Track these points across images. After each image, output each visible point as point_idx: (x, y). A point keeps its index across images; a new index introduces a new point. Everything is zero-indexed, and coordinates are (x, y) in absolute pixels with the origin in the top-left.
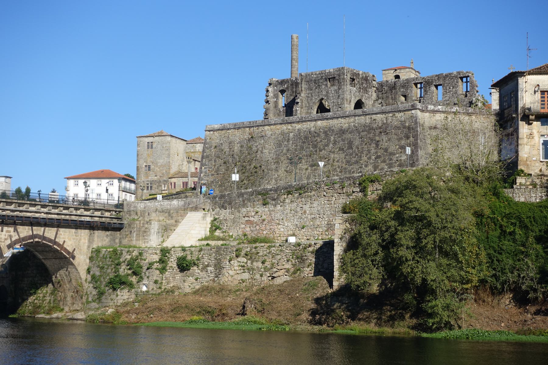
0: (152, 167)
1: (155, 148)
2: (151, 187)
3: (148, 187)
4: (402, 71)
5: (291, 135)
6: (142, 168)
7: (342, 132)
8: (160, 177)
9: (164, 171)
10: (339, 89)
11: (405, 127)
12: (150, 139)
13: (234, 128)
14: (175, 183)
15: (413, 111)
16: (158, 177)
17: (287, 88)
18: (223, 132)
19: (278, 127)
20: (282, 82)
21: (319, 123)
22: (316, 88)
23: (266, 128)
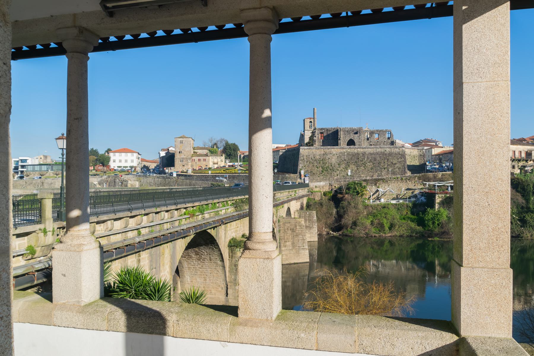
0: (183, 152)
2: (183, 161)
3: (181, 161)
7: (371, 154)
10: (360, 136)
11: (399, 154)
12: (181, 139)
13: (316, 149)
14: (194, 159)
15: (403, 149)
17: (324, 131)
20: (322, 129)
21: (359, 150)
22: (348, 134)
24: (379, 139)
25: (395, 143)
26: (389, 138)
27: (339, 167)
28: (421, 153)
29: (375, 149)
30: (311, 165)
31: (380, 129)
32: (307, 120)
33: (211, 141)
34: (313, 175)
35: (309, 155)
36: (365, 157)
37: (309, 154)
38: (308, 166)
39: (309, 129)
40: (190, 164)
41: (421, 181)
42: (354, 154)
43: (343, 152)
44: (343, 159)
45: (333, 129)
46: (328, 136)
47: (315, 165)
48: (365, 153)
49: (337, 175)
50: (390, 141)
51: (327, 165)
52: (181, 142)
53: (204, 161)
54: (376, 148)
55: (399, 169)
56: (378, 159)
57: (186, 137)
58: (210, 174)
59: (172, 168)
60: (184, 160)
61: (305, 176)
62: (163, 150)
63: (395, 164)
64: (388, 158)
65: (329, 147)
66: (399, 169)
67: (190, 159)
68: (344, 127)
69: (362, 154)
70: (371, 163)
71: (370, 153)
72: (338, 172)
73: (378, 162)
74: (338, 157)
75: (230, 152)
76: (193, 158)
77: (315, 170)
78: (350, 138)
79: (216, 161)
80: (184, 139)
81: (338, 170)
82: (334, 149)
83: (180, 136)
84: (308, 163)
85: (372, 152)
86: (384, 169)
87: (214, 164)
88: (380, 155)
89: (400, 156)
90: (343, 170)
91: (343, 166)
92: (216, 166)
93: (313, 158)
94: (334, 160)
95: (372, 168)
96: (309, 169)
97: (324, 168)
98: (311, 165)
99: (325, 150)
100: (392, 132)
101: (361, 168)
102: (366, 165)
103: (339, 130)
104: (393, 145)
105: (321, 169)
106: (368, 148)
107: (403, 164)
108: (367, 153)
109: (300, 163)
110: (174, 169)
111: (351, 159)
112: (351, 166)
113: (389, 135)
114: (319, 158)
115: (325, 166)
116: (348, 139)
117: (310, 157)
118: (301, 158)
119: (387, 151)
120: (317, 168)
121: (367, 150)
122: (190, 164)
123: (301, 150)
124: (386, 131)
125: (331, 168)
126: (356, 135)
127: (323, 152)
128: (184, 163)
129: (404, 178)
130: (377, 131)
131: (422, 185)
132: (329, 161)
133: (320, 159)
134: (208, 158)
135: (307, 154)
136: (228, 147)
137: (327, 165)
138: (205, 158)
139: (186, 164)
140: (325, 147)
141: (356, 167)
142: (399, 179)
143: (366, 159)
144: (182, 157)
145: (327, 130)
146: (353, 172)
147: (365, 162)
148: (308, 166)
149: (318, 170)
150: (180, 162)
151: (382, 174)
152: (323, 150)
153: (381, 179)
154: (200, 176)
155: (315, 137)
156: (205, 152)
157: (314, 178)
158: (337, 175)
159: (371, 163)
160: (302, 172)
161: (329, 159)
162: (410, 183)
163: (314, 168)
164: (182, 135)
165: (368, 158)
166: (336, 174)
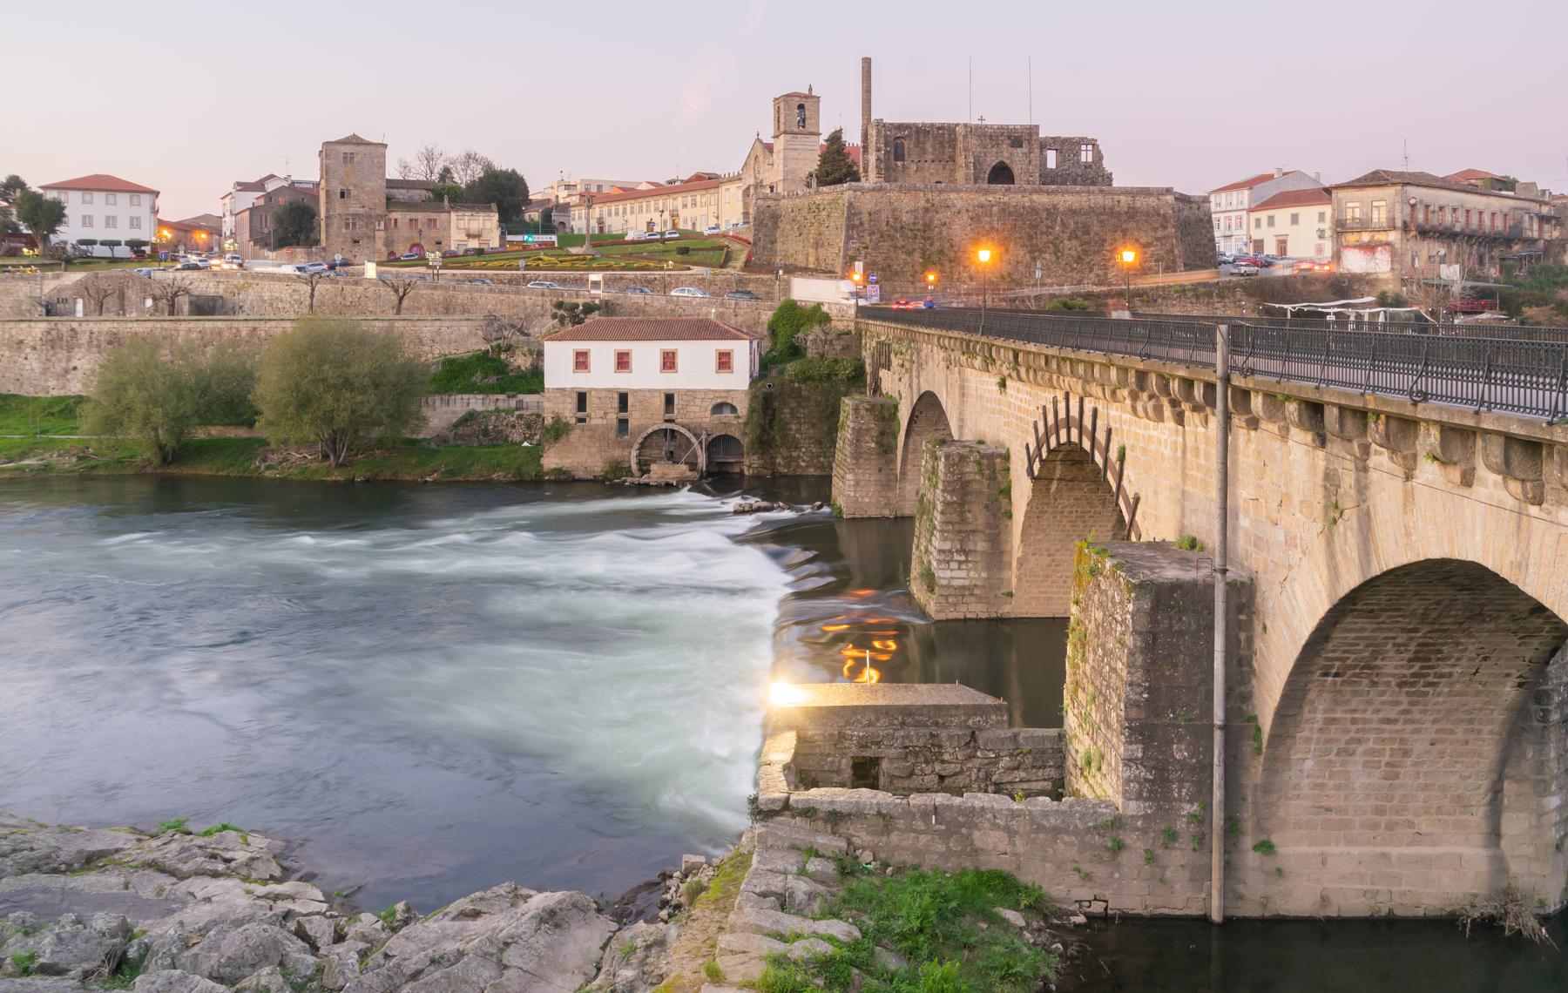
0: (354, 192)
1: (359, 163)
2: (354, 224)
3: (348, 224)
5: (995, 209)
6: (335, 194)
7: (1073, 212)
8: (370, 209)
9: (377, 201)
10: (1030, 153)
12: (348, 149)
14: (396, 220)
17: (909, 136)
21: (1035, 197)
22: (993, 147)
23: (953, 196)
31: (1064, 135)
36: (1056, 220)
43: (988, 203)
48: (1055, 207)
54: (1089, 192)
60: (360, 223)
67: (380, 218)
69: (1047, 210)
71: (1071, 210)
78: (1000, 159)
80: (361, 148)
85: (1076, 206)
87: (469, 236)
92: (474, 244)
95: (1079, 257)
101: (1044, 255)
108: (1061, 209)
113: (1090, 154)
116: (991, 161)
122: (380, 235)
127: (922, 203)
130: (1054, 139)
133: (915, 224)
134: (444, 216)
139: (368, 237)
141: (1030, 252)
143: (1057, 228)
144: (351, 210)
147: (1056, 239)
150: (344, 230)
151: (1109, 276)
159: (1075, 242)
165: (1063, 224)
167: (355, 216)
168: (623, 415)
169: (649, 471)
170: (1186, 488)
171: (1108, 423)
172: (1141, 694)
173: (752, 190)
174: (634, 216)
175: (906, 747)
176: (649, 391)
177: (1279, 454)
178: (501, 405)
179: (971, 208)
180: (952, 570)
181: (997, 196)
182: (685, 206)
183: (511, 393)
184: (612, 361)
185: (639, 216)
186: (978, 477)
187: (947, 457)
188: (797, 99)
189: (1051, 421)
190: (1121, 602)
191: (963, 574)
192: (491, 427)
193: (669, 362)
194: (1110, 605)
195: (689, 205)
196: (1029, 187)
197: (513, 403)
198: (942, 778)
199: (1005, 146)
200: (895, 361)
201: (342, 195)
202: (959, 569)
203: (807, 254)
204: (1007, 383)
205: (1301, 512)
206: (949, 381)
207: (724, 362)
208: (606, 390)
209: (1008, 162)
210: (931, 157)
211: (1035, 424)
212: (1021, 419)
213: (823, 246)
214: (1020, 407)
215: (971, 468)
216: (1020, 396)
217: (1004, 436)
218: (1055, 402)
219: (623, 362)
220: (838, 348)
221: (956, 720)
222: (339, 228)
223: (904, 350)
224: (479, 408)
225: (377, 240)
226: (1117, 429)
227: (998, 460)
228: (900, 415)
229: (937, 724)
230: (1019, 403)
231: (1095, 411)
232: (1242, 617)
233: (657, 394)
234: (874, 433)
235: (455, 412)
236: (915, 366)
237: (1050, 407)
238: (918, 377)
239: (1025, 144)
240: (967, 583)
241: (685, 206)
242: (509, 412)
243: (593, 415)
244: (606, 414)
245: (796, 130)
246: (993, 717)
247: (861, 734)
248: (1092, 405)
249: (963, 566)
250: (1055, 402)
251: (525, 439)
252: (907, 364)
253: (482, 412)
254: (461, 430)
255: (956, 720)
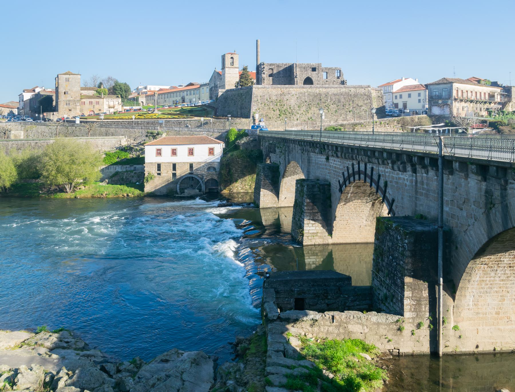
2: (69, 104)
3: (67, 104)
4: (235, 55)
5: (306, 94)
7: (335, 95)
10: (318, 73)
11: (365, 95)
12: (67, 76)
14: (84, 102)
16: (73, 98)
17: (274, 68)
18: (265, 89)
19: (298, 89)
20: (271, 65)
21: (321, 89)
24: (328, 79)
25: (346, 83)
26: (338, 78)
27: (300, 110)
28: (379, 94)
29: (339, 89)
30: (267, 107)
31: (329, 67)
32: (228, 55)
33: (95, 80)
34: (269, 119)
35: (264, 96)
37: (264, 94)
38: (263, 109)
39: (230, 66)
40: (78, 108)
41: (400, 125)
42: (316, 95)
43: (303, 92)
44: (303, 101)
45: (285, 65)
46: (279, 73)
47: (271, 108)
49: (297, 120)
50: (339, 80)
51: (285, 107)
52: (67, 80)
53: (90, 104)
55: (366, 111)
56: (342, 100)
57: (73, 73)
58: (134, 120)
59: (55, 113)
60: (71, 103)
61: (260, 121)
62: (28, 91)
63: (361, 106)
64: (353, 99)
65: (287, 86)
66: (366, 111)
67: (78, 101)
68: (301, 63)
69: (325, 94)
70: (335, 106)
71: (334, 94)
72: (298, 116)
73: (343, 104)
74: (297, 98)
75: (121, 93)
76: (83, 100)
77: (271, 114)
79: (111, 104)
80: (71, 76)
81: (298, 113)
82: (292, 88)
83: (64, 72)
84: (263, 105)
86: (350, 112)
87: (110, 107)
88: (345, 96)
89: (366, 97)
90: (304, 113)
91: (304, 108)
92: (112, 110)
93: (268, 99)
94: (293, 102)
95: (336, 111)
96: (264, 113)
97: (282, 111)
98: (267, 107)
99: (282, 89)
100: (342, 71)
102: (330, 108)
103: (295, 66)
104: (344, 84)
105: (278, 112)
106: (331, 88)
107: (369, 107)
108: (330, 94)
109: (253, 105)
110: (58, 115)
111: (313, 100)
112: (312, 108)
113: (339, 73)
114: (276, 99)
115: (283, 109)
116: (305, 77)
117: (266, 97)
118: (254, 99)
119: (352, 91)
120: (274, 111)
121: (329, 89)
123: (254, 89)
124: (335, 69)
125: (290, 111)
126: (314, 72)
128: (70, 107)
129: (383, 122)
130: (326, 68)
131: (401, 130)
132: (288, 103)
133: (277, 100)
135: (261, 94)
136: (118, 87)
137: (285, 107)
138: (98, 100)
139: (74, 108)
140: (282, 86)
142: (378, 123)
143: (329, 100)
144: (68, 99)
145: (278, 66)
146: (315, 115)
147: (328, 104)
148: (263, 109)
149: (275, 113)
150: (65, 106)
151: (348, 117)
152: (280, 89)
153: (359, 124)
154: (109, 123)
155: (264, 73)
156: (92, 93)
157: (270, 124)
158: (297, 120)
159: (335, 106)
160: (257, 116)
161: (287, 100)
162: (389, 127)
163: (269, 111)
164: (67, 71)
165: (331, 99)
166: (295, 118)
167: (69, 101)
168: (174, 172)
169: (184, 192)
170: (417, 196)
171: (379, 173)
172: (411, 273)
173: (213, 89)
174: (168, 99)
175: (315, 294)
176: (184, 163)
177: (463, 184)
178: (128, 169)
179: (297, 94)
180: (310, 227)
181: (307, 89)
182: (187, 95)
183: (131, 165)
184: (170, 152)
185: (170, 99)
186: (319, 193)
187: (308, 185)
188: (230, 55)
189: (351, 171)
190: (401, 239)
191: (314, 228)
192: (124, 177)
193: (191, 152)
194: (395, 240)
195: (189, 94)
196: (318, 86)
197: (132, 168)
198: (328, 305)
199: (309, 71)
200: (278, 150)
201: (65, 93)
202: (312, 226)
203: (238, 112)
204: (329, 158)
205: (474, 205)
206: (303, 158)
207: (211, 151)
208: (168, 163)
209: (310, 77)
210: (282, 75)
211: (343, 173)
212: (336, 171)
213: (243, 108)
214: (335, 167)
215: (316, 189)
216: (335, 163)
217: (328, 177)
218: (353, 165)
219: (174, 152)
220: (252, 146)
221: (332, 284)
222: (63, 105)
223: (282, 146)
224: (120, 170)
225: (77, 109)
226: (383, 175)
227: (326, 186)
228: (280, 170)
229: (325, 285)
230: (335, 165)
231: (372, 169)
232: (447, 244)
233: (187, 164)
234: (270, 177)
235: (111, 172)
236: (287, 152)
237: (350, 167)
238: (288, 156)
239: (317, 70)
240: (315, 231)
241: (187, 95)
242: (131, 171)
243: (163, 172)
244: (168, 172)
245: (230, 66)
246: (346, 282)
247: (298, 290)
248: (371, 166)
249: (314, 225)
250: (353, 165)
251: (137, 182)
252: (283, 152)
253: (121, 172)
254: (113, 179)
255: (332, 284)
